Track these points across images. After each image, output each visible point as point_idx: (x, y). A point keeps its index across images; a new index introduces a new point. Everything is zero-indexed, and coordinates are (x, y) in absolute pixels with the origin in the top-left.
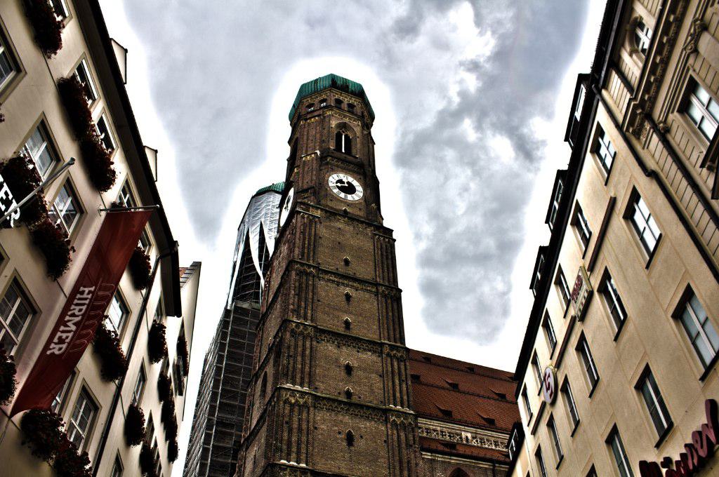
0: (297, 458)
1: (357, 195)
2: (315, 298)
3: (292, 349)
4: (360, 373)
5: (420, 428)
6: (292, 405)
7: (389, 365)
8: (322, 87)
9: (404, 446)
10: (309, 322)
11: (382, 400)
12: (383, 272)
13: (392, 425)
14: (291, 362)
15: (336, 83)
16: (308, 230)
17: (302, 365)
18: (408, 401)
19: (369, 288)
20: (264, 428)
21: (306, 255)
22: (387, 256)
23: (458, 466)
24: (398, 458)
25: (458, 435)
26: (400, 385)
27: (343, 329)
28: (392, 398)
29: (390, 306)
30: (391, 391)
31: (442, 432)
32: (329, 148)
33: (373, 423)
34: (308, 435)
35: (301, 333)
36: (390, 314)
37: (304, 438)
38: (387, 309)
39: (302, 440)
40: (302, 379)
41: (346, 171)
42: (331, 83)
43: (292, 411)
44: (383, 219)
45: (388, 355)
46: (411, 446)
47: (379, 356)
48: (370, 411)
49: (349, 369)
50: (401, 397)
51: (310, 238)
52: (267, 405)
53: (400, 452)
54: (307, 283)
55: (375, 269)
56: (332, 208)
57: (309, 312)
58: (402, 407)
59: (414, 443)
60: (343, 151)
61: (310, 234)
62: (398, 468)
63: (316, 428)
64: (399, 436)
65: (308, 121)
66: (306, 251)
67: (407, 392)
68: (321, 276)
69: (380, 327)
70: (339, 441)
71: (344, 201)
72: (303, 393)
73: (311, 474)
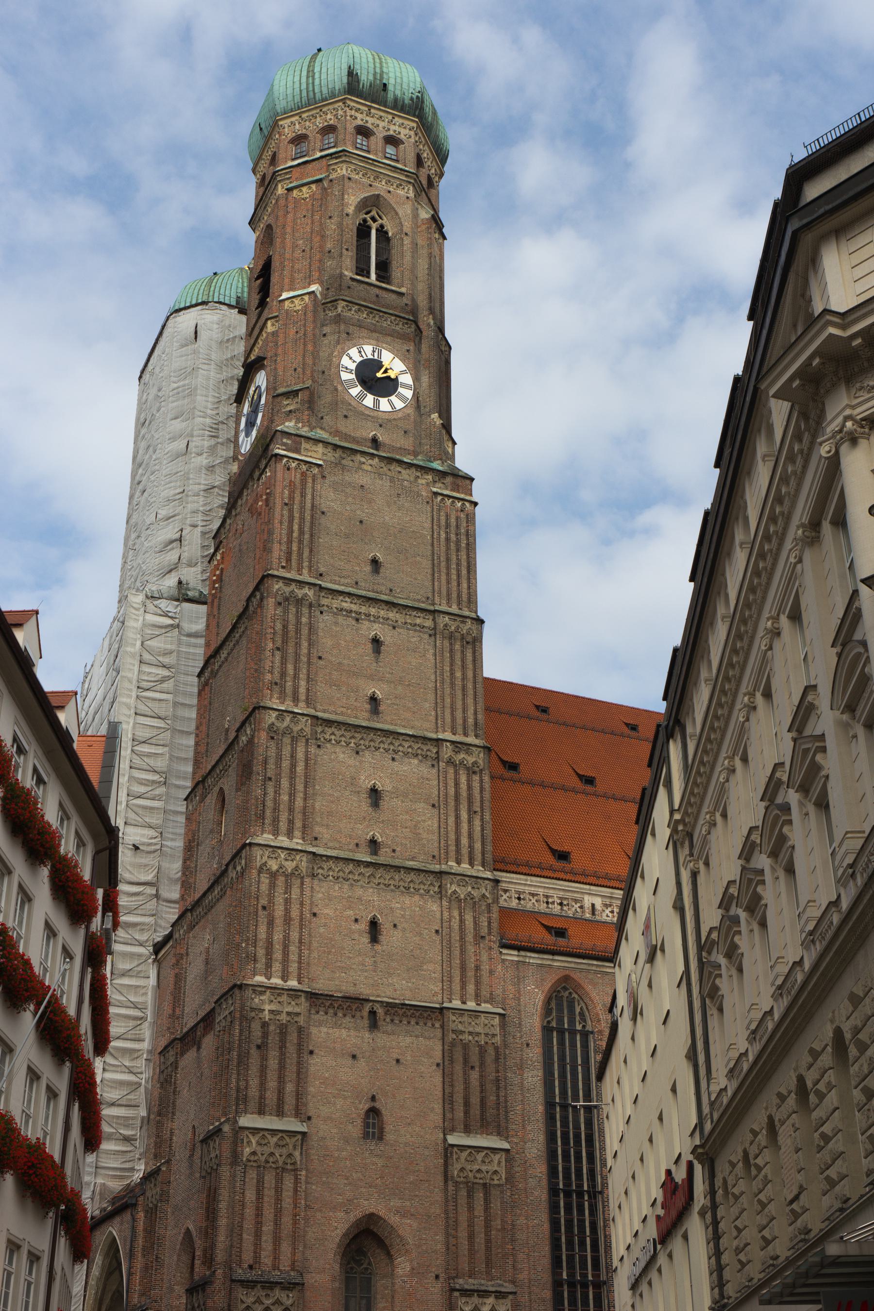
0: (283, 971)
1: (402, 398)
2: (315, 654)
3: (271, 766)
4: (396, 802)
5: (506, 891)
6: (273, 875)
7: (451, 783)
8: (325, 91)
9: (470, 938)
10: (302, 704)
11: (436, 853)
12: (448, 582)
13: (450, 902)
14: (271, 790)
15: (358, 82)
17: (290, 795)
18: (483, 854)
19: (418, 621)
20: (222, 907)
21: (294, 557)
22: (458, 542)
23: (567, 972)
24: (458, 962)
25: (576, 901)
26: (470, 821)
27: (366, 715)
28: (453, 848)
30: (452, 836)
31: (547, 897)
32: (341, 275)
33: (417, 898)
34: (301, 929)
35: (288, 731)
36: (458, 674)
37: (295, 935)
38: (452, 664)
39: (292, 938)
40: (291, 822)
41: (379, 334)
42: (345, 80)
43: (272, 886)
44: (454, 443)
45: (450, 762)
46: (483, 937)
47: (433, 766)
48: (412, 876)
49: (375, 794)
50: (471, 847)
51: (302, 519)
52: (227, 865)
53: (463, 951)
54: (298, 622)
55: (433, 575)
56: (346, 437)
57: (303, 683)
58: (471, 864)
60: (373, 276)
62: (457, 979)
63: (315, 915)
64: (462, 921)
65: (295, 193)
66: (295, 548)
67: (482, 835)
68: (324, 601)
69: (436, 703)
70: (356, 936)
71: (373, 416)
73: (306, 998)
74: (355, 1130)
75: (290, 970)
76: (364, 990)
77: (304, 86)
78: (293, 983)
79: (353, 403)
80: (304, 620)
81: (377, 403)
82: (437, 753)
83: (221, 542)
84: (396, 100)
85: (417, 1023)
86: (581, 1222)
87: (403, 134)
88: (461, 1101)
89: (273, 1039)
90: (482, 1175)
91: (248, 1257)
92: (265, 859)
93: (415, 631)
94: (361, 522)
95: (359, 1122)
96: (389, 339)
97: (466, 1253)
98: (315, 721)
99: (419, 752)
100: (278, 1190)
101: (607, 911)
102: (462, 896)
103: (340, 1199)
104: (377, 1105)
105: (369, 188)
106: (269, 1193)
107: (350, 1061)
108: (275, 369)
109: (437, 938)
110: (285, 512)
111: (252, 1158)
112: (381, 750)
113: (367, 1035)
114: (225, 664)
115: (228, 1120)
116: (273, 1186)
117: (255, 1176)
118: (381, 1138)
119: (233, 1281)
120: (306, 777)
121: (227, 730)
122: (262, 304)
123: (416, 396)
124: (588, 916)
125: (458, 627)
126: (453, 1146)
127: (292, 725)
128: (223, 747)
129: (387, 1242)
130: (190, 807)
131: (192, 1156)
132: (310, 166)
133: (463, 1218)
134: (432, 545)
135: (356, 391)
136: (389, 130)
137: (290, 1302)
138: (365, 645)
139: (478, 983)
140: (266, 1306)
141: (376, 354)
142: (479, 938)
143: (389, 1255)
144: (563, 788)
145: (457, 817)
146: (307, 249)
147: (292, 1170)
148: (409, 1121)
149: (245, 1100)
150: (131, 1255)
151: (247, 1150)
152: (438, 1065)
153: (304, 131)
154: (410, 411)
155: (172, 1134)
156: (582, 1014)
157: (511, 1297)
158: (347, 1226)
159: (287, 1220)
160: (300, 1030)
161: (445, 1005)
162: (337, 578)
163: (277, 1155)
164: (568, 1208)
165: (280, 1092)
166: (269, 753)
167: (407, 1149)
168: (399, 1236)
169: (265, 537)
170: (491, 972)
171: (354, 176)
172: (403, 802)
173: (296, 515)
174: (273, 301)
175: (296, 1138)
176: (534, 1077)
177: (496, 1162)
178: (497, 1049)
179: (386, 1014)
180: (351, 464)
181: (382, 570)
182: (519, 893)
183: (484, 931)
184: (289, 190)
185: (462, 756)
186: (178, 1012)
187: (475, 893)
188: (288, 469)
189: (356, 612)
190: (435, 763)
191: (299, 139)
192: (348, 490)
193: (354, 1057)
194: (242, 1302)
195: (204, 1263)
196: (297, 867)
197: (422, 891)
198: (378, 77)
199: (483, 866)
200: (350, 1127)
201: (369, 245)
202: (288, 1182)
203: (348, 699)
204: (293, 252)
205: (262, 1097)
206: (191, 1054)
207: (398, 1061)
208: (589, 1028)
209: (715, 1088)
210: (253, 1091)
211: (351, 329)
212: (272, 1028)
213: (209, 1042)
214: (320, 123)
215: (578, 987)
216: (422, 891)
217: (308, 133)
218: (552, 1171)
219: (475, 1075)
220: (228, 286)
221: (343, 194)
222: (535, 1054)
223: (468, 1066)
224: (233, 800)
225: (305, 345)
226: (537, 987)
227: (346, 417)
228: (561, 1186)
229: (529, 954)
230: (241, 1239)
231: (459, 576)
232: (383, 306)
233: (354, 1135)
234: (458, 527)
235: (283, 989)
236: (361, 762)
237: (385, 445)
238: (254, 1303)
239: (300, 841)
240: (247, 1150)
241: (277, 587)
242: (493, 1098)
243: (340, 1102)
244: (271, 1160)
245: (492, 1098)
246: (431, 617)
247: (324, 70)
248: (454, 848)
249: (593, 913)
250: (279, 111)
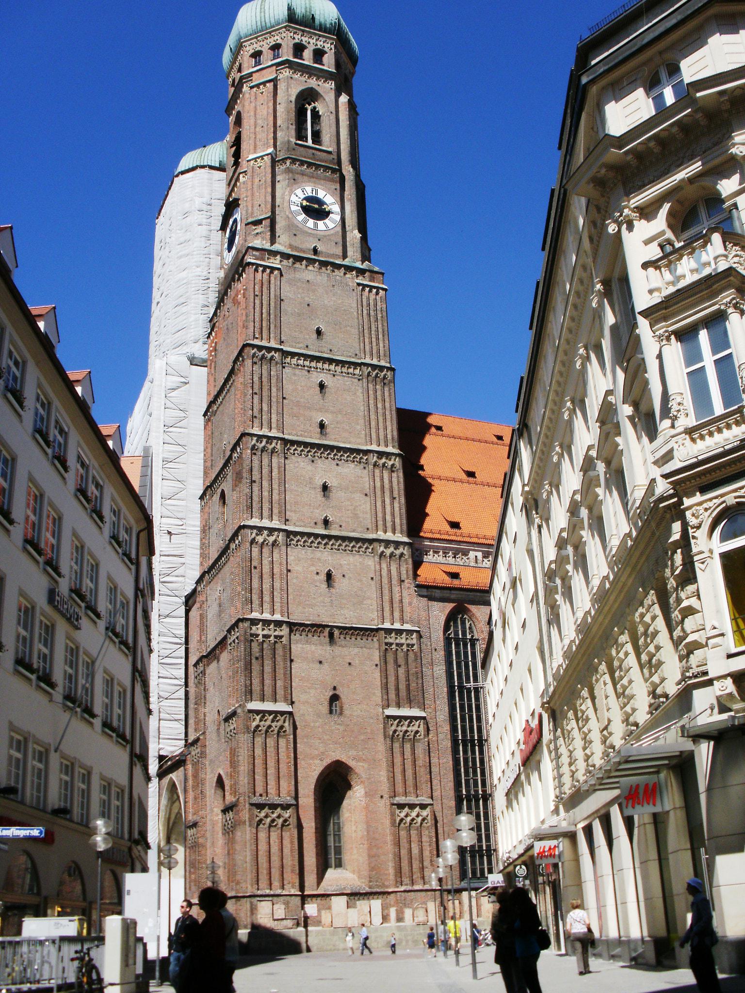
1: (333, 221)
4: (341, 494)
7: (378, 479)
8: (273, 21)
9: (395, 581)
11: (370, 527)
15: (295, 14)
26: (392, 504)
27: (318, 435)
28: (380, 523)
29: (379, 393)
30: (380, 515)
32: (289, 142)
33: (357, 557)
35: (263, 450)
36: (380, 405)
42: (286, 13)
46: (403, 581)
47: (365, 468)
53: (391, 591)
58: (394, 533)
63: (289, 571)
64: (389, 571)
67: (400, 513)
70: (318, 584)
72: (271, 531)
74: (325, 708)
76: (326, 620)
77: (258, 19)
78: (277, 617)
79: (300, 226)
81: (316, 225)
82: (366, 459)
83: (214, 324)
84: (320, 25)
86: (474, 760)
87: (327, 46)
89: (267, 653)
93: (349, 377)
94: (308, 305)
95: (326, 704)
96: (322, 182)
97: (400, 781)
103: (316, 752)
104: (337, 692)
105: (305, 84)
106: (271, 750)
107: (318, 665)
108: (247, 206)
109: (373, 583)
110: (257, 302)
112: (329, 459)
113: (329, 648)
114: (221, 406)
115: (240, 705)
118: (341, 714)
121: (224, 451)
122: (236, 164)
123: (343, 220)
124: (472, 564)
125: (377, 374)
126: (388, 717)
128: (223, 462)
130: (203, 504)
131: (218, 729)
132: (265, 71)
133: (398, 760)
134: (358, 318)
135: (302, 217)
136: (317, 45)
137: (287, 815)
138: (315, 388)
141: (314, 192)
144: (454, 480)
145: (384, 502)
146: (265, 126)
148: (359, 702)
149: (251, 692)
150: (185, 791)
151: (254, 724)
152: (377, 665)
153: (260, 49)
154: (339, 229)
155: (205, 715)
156: (470, 628)
157: (429, 807)
158: (321, 769)
160: (284, 647)
161: (380, 626)
162: (294, 344)
164: (465, 752)
168: (356, 773)
169: (244, 318)
170: (410, 604)
171: (293, 76)
173: (265, 302)
174: (243, 161)
176: (440, 670)
179: (340, 634)
180: (300, 266)
181: (324, 337)
183: (404, 577)
184: (252, 88)
185: (384, 460)
186: (203, 638)
189: (307, 367)
190: (366, 465)
191: (257, 55)
192: (298, 284)
193: (320, 662)
194: (257, 816)
195: (231, 794)
197: (361, 553)
198: (308, 10)
199: (401, 534)
200: (320, 707)
201: (306, 121)
204: (255, 127)
206: (214, 665)
207: (350, 664)
208: (476, 637)
209: (555, 665)
210: (256, 687)
211: (296, 176)
212: (265, 646)
213: (225, 656)
214: (272, 42)
216: (361, 553)
217: (262, 49)
218: (454, 729)
219: (402, 671)
220: (214, 154)
221: (288, 89)
222: (440, 655)
224: (230, 496)
225: (266, 188)
227: (295, 235)
228: (460, 738)
230: (254, 778)
231: (377, 339)
232: (317, 160)
234: (376, 305)
237: (322, 252)
239: (278, 522)
241: (253, 351)
243: (313, 691)
246: (359, 368)
247: (271, 7)
249: (476, 562)
250: (242, 36)
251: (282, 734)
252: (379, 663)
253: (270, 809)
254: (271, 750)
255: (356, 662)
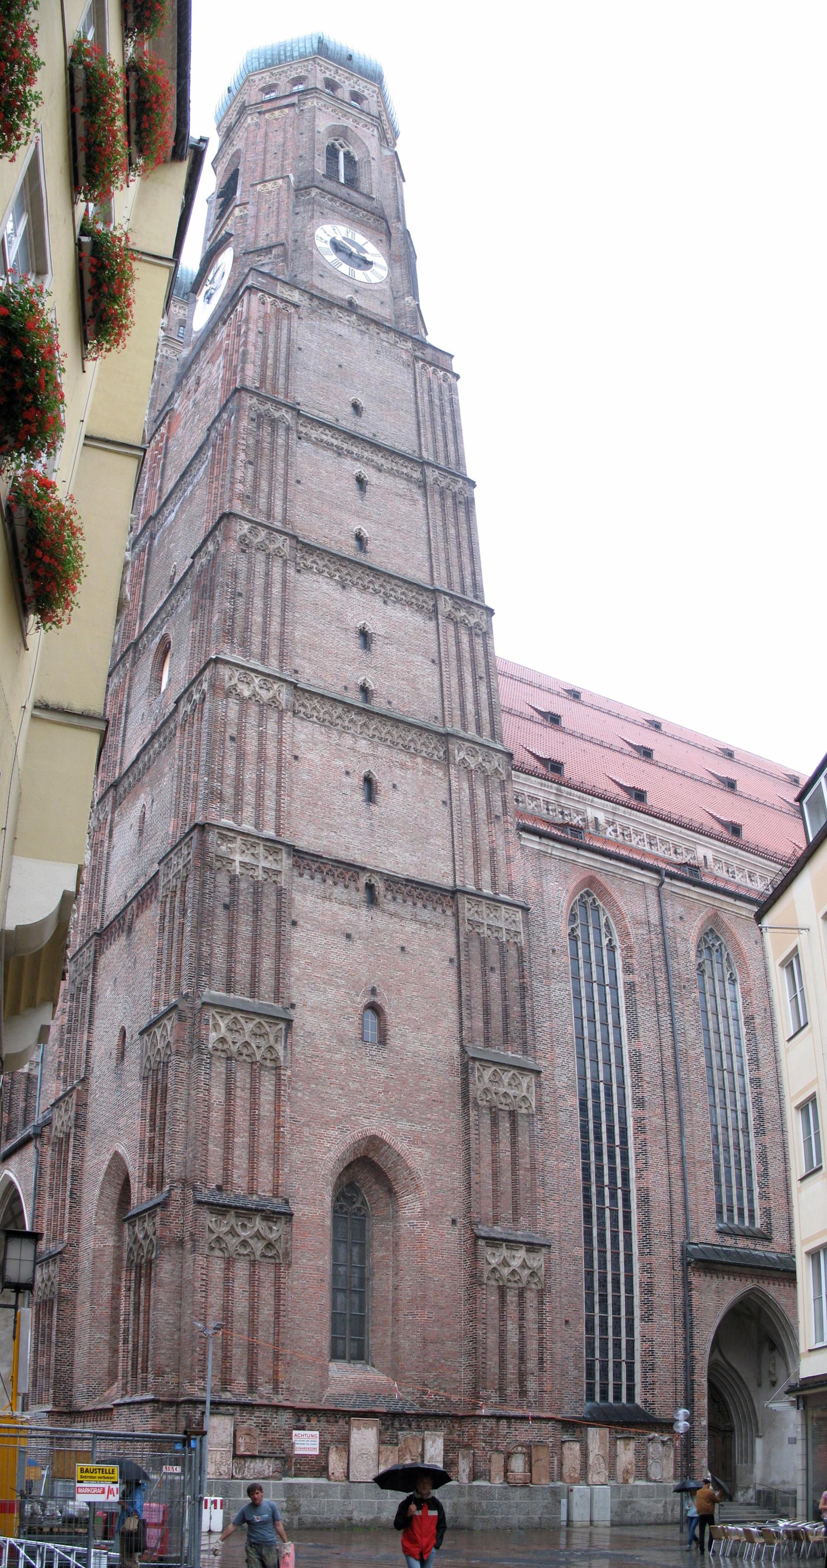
4: (391, 649)
6: (243, 701)
7: (452, 641)
9: (482, 815)
13: (459, 771)
16: (272, 328)
23: (592, 873)
25: (578, 813)
37: (271, 777)
39: (268, 780)
40: (265, 646)
46: (497, 817)
47: (430, 619)
49: (365, 636)
50: (478, 713)
59: (505, 813)
61: (277, 338)
63: (296, 758)
64: (473, 795)
73: (289, 854)
75: (267, 818)
76: (359, 858)
80: (281, 441)
85: (425, 907)
88: (480, 1008)
89: (245, 899)
90: (509, 1101)
91: (215, 1175)
92: (234, 681)
95: (356, 1019)
98: (294, 542)
99: (414, 600)
100: (254, 1091)
101: (610, 829)
102: (473, 766)
103: (333, 1114)
104: (378, 1000)
106: (241, 1095)
107: (344, 941)
111: (220, 1046)
113: (364, 911)
116: (248, 1086)
117: (223, 1070)
119: (199, 1203)
120: (284, 600)
126: (474, 1059)
127: (267, 542)
129: (391, 1176)
139: (494, 870)
140: (242, 1239)
142: (493, 818)
143: (391, 1192)
145: (461, 679)
147: (272, 1068)
149: (209, 971)
151: (213, 1036)
156: (607, 925)
158: (343, 1149)
159: (266, 1133)
160: (280, 892)
163: (253, 1045)
165: (254, 967)
166: (240, 567)
167: (416, 1059)
172: (398, 650)
175: (279, 1027)
177: (525, 1085)
178: (520, 950)
182: (518, 794)
185: (463, 613)
187: (486, 765)
188: (263, 303)
193: (348, 936)
194: (211, 1231)
196: (274, 697)
200: (345, 1024)
202: (267, 1083)
203: (331, 528)
205: (230, 970)
207: (403, 949)
210: (219, 962)
212: (243, 885)
215: (604, 893)
219: (495, 979)
223: (486, 969)
226: (561, 885)
229: (551, 843)
233: (350, 1034)
235: (258, 838)
236: (348, 598)
238: (227, 1233)
240: (213, 1036)
242: (517, 1009)
243: (331, 992)
244: (245, 1051)
245: (515, 1009)
248: (459, 713)
251: (268, 1063)
252: (454, 957)
253: (238, 1215)
254: (241, 1095)
255: (413, 947)
